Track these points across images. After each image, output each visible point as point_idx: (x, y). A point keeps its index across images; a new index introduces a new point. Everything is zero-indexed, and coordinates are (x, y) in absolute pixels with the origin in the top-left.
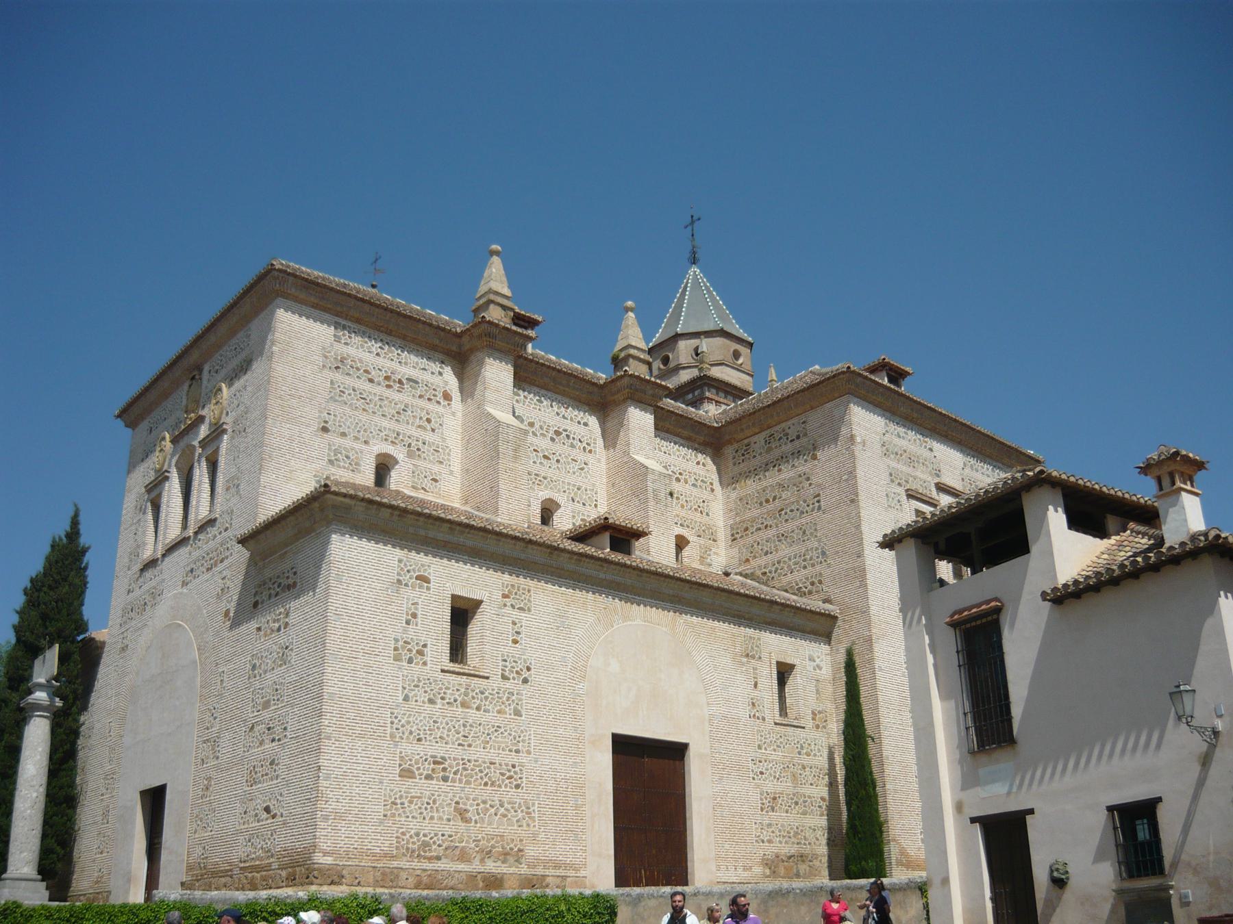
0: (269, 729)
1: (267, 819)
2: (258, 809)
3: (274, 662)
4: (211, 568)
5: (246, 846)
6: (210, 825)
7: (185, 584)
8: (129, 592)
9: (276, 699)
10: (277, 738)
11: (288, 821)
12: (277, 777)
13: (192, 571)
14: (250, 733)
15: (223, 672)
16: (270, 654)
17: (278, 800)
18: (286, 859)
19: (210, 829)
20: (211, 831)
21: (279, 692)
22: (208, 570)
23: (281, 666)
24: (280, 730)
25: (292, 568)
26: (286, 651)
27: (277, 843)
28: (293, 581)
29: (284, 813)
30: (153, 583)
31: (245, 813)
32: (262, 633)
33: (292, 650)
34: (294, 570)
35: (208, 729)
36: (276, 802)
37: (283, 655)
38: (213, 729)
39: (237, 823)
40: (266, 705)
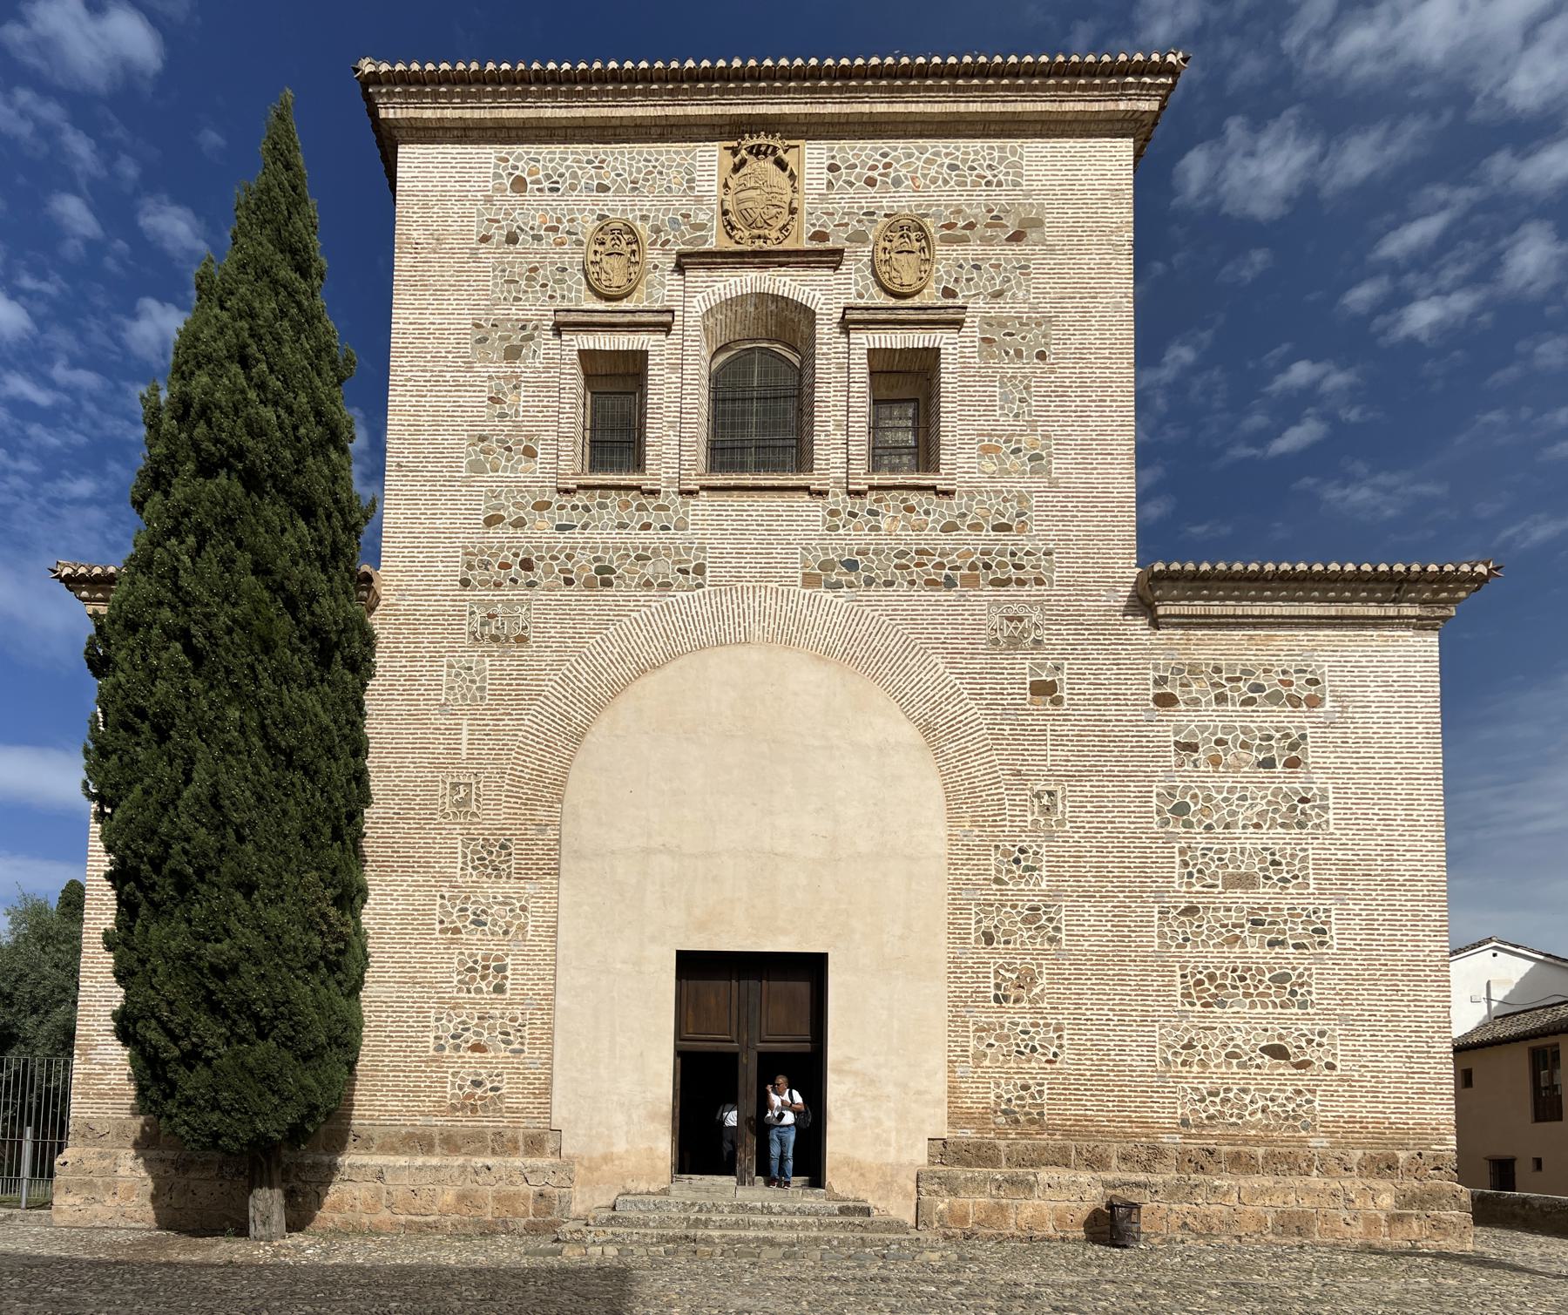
0: (1255, 922)
1: (1278, 1066)
2: (1235, 1046)
3: (1260, 814)
4: (950, 583)
5: (1202, 1100)
6: (1040, 1050)
7: (810, 581)
8: (491, 521)
9: (1276, 878)
10: (1291, 942)
11: (1357, 1078)
12: (1303, 1005)
13: (852, 565)
14: (1182, 918)
15: (1050, 794)
16: (1243, 798)
17: (1310, 1042)
18: (1357, 1135)
19: (1044, 1059)
20: (1049, 1062)
21: (1284, 867)
22: (928, 582)
23: (1283, 825)
24: (1300, 931)
25: (1305, 671)
26: (1301, 806)
27: (1318, 1108)
28: (1306, 693)
29: (1338, 1064)
30: (637, 538)
31: (1189, 1046)
32: (1200, 756)
33: (1325, 808)
34: (1309, 676)
35: (998, 881)
36: (1304, 1044)
37: (1293, 809)
38: (1022, 886)
39: (1158, 1060)
40: (1245, 881)
